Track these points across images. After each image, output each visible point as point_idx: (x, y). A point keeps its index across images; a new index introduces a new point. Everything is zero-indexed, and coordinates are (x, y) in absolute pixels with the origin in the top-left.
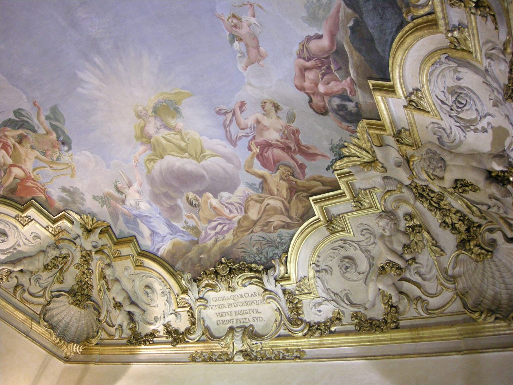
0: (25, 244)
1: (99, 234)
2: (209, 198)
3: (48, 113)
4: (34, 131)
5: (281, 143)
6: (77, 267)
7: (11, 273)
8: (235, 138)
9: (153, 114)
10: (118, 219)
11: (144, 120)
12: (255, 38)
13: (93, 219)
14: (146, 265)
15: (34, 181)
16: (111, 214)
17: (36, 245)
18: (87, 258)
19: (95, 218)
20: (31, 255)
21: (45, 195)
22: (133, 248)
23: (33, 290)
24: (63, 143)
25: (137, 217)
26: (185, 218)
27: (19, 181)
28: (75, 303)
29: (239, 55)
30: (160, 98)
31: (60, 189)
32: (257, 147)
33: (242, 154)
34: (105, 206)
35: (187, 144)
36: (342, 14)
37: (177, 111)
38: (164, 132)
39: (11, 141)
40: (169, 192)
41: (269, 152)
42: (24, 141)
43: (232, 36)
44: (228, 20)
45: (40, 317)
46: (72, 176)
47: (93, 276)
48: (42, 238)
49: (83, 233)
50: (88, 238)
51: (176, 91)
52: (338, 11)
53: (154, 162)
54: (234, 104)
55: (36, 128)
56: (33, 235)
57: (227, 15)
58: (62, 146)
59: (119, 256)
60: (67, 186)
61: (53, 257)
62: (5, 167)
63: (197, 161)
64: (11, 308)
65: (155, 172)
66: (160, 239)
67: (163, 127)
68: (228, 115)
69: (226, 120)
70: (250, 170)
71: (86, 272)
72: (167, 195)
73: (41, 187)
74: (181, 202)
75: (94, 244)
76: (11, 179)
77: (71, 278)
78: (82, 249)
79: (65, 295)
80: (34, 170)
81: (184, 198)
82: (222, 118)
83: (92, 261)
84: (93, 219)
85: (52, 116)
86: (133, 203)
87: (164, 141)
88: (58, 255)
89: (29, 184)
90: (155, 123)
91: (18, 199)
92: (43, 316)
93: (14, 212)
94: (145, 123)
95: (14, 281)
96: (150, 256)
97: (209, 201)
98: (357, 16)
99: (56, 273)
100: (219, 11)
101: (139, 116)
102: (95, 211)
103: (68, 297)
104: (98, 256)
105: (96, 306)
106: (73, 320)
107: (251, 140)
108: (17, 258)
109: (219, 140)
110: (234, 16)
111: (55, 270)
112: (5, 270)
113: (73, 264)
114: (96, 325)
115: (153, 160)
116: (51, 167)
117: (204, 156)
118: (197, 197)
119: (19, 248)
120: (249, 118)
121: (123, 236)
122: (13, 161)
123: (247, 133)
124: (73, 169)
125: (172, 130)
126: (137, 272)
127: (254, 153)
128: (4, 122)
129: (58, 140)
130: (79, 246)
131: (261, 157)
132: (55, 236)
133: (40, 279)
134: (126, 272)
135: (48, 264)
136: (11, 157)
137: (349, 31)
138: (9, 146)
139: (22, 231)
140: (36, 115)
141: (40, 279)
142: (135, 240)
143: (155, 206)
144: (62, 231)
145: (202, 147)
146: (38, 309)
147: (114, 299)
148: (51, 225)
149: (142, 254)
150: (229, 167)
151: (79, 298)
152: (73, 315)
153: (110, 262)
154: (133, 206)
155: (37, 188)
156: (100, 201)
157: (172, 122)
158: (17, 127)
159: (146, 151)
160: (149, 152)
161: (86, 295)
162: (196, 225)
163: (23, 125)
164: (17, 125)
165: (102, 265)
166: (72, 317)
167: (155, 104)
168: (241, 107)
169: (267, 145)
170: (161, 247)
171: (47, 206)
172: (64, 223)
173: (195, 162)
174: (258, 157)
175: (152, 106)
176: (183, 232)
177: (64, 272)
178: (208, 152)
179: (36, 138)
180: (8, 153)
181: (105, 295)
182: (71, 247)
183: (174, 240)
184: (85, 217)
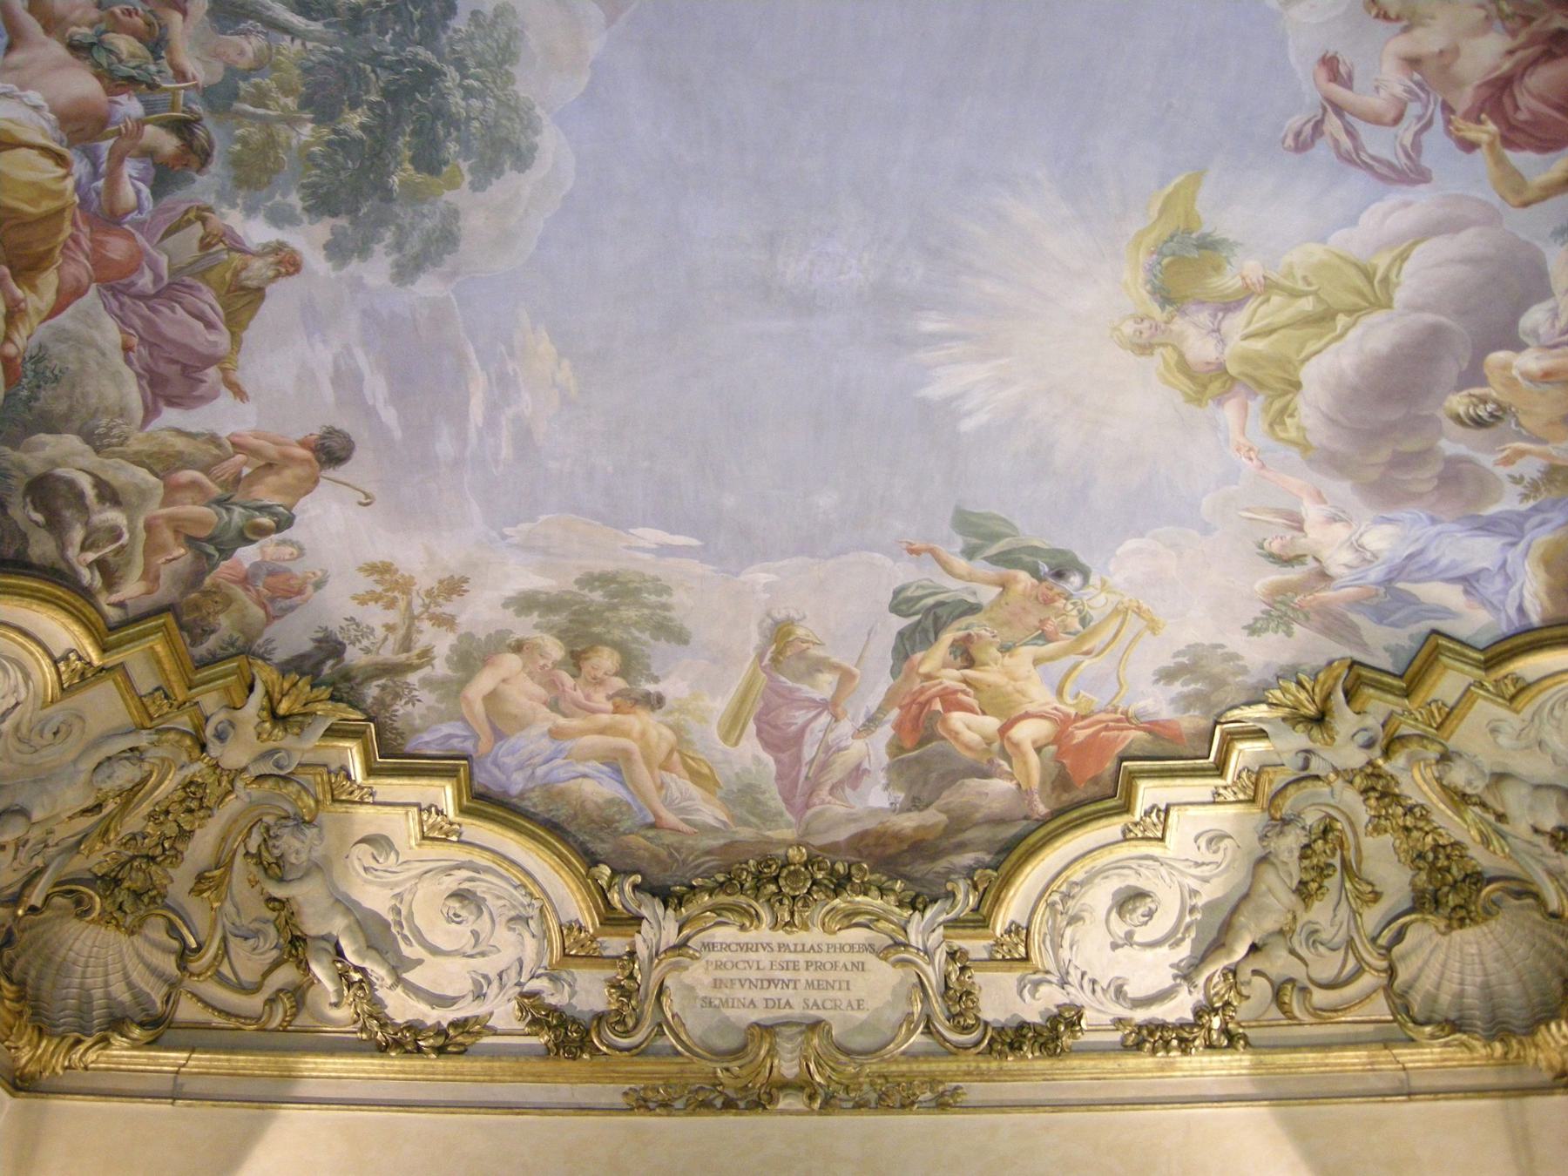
0: (1205, 880)
1: (1348, 702)
2: (1506, 367)
3: (959, 542)
4: (974, 609)
5: (1523, 47)
6: (1378, 830)
7: (1235, 974)
8: (1404, 160)
9: (1169, 308)
10: (1354, 628)
11: (1164, 345)
13: (1300, 684)
14: (1530, 678)
15: (1084, 717)
16: (1327, 631)
17: (1233, 860)
18: (1378, 788)
19: (1302, 677)
20: (1244, 890)
21: (1138, 728)
22: (1458, 665)
23: (1326, 972)
24: (1059, 575)
25: (1390, 580)
26: (1502, 472)
27: (1053, 748)
28: (1455, 923)
30: (1143, 258)
31: (1157, 681)
32: (1479, 122)
33: (1465, 177)
34: (1296, 627)
35: (1315, 293)
37: (1208, 245)
38: (1236, 323)
39: (951, 678)
40: (1400, 448)
41: (1524, 100)
42: (974, 652)
45: (1401, 1025)
46: (1153, 627)
47: (1437, 819)
48: (1229, 832)
49: (1310, 737)
50: (1333, 739)
51: (1157, 205)
53: (1292, 416)
54: (1310, 87)
55: (971, 599)
56: (1203, 842)
58: (1062, 583)
59: (1448, 714)
60: (1169, 662)
61: (1296, 854)
62: (996, 746)
63: (1381, 307)
64: (1311, 1057)
65: (1320, 435)
66: (1499, 583)
67: (1220, 315)
68: (1327, 127)
69: (1336, 142)
70: (1529, 195)
71: (1409, 821)
72: (1402, 462)
73: (1113, 716)
74: (1454, 444)
75: (1362, 738)
76: (1033, 759)
77: (1387, 866)
78: (1348, 776)
79: (1412, 922)
80: (1060, 693)
81: (1449, 424)
82: (1322, 149)
83: (1397, 784)
84: (1300, 684)
85: (974, 541)
86: (1347, 556)
87: (1259, 345)
88: (1305, 841)
89: (1080, 735)
90: (1196, 325)
91: (1094, 790)
92: (1409, 1017)
93: (1111, 829)
94: (1175, 348)
95: (1261, 988)
96: (1518, 646)
97: (1515, 372)
99: (1342, 885)
101: (1145, 349)
102: (1285, 658)
103: (1425, 921)
104: (1399, 760)
105: (1514, 886)
106: (1492, 966)
107: (1448, 122)
108: (1217, 925)
109: (1377, 204)
111: (1332, 883)
112: (1216, 979)
113: (1361, 830)
114: (1557, 931)
115: (1283, 411)
116: (1087, 653)
117: (1385, 280)
118: (1477, 391)
119: (1200, 901)
120: (1381, 76)
121: (1405, 658)
122: (996, 715)
123: (1420, 118)
124: (1139, 612)
125: (1246, 299)
126: (1527, 712)
127: (1491, 145)
128: (895, 649)
129: (1041, 580)
130: (1332, 776)
131: (1514, 135)
132: (1252, 801)
133: (1316, 931)
134: (1503, 740)
135: (1302, 883)
136: (984, 713)
138: (955, 692)
139: (1170, 854)
140: (940, 570)
141: (1316, 931)
142: (1443, 642)
143: (1406, 513)
144: (1259, 774)
145: (1356, 265)
146: (1380, 1008)
147: (1536, 831)
148: (1219, 782)
149: (1492, 658)
150: (1469, 240)
151: (1452, 900)
152: (1480, 954)
153: (1438, 748)
154: (1355, 563)
155: (1107, 728)
156: (1273, 625)
157: (1228, 281)
158: (932, 636)
159: (1245, 408)
160: (1255, 405)
161: (1464, 880)
162: (1545, 462)
163: (937, 619)
164: (925, 631)
165: (1435, 771)
166: (1482, 963)
167: (1147, 282)
168: (1335, 76)
169: (1498, 94)
170: (1522, 596)
171: (1170, 748)
172: (1245, 753)
173: (1378, 316)
174: (1508, 143)
175: (1147, 296)
176: (1535, 509)
177: (1359, 869)
178: (1382, 262)
179: (990, 619)
180: (971, 710)
181: (1510, 839)
182: (1319, 795)
183: (1536, 552)
184: (1278, 693)
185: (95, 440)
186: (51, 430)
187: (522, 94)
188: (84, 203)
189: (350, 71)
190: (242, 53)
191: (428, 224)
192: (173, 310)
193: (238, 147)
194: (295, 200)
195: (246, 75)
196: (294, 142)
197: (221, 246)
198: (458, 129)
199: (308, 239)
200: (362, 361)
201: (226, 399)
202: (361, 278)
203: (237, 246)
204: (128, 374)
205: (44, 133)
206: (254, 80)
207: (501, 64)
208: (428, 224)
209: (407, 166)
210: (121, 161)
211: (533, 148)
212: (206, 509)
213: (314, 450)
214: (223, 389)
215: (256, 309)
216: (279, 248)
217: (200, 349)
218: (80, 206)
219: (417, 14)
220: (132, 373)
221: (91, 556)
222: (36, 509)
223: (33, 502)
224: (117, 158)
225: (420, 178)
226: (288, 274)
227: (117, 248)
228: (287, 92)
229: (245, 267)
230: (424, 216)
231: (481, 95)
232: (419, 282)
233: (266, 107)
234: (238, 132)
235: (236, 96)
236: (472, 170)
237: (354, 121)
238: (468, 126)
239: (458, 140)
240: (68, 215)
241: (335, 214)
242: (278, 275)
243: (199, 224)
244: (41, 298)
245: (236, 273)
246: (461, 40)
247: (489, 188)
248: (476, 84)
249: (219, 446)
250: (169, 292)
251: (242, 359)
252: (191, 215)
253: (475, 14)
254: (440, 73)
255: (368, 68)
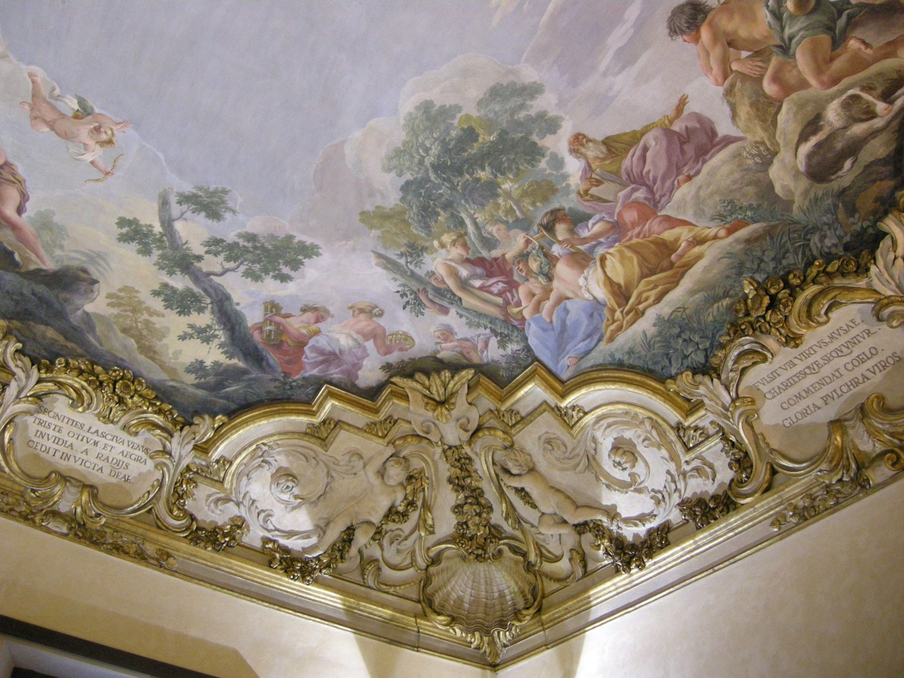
12: (66, 136)
29: (57, 92)
36: (33, 257)
43: (89, 110)
44: (111, 129)
52: (38, 256)
57: (119, 137)
98: (23, 270)
100: (130, 131)
110: (110, 142)
137: (10, 248)
185: (767, 158)
186: (771, 187)
187: (404, 133)
188: (616, 241)
189: (467, 192)
190: (499, 229)
191: (497, 107)
192: (649, 171)
193: (538, 204)
194: (543, 164)
195: (506, 223)
196: (516, 186)
197: (594, 176)
198: (445, 139)
199: (558, 143)
200: (606, 61)
201: (692, 107)
202: (556, 105)
203: (589, 168)
204: (706, 169)
205: (596, 269)
206: (505, 219)
207: (404, 151)
208: (497, 107)
209: (480, 140)
210: (584, 238)
211: (417, 108)
212: (798, 55)
213: (698, 28)
214: (685, 113)
215: (618, 136)
216: (574, 151)
217: (664, 143)
218: (620, 241)
219: (423, 191)
220: (705, 166)
221: (880, 106)
222: (841, 169)
223: (833, 174)
224: (585, 240)
225: (480, 131)
226: (584, 136)
227: (630, 216)
228: (498, 206)
229: (597, 158)
230: (495, 113)
231: (422, 145)
232: (533, 80)
233: (511, 207)
234: (531, 208)
235: (517, 220)
236: (454, 117)
237: (484, 175)
238: (439, 137)
239: (448, 134)
240: (628, 244)
241: (535, 144)
242: (589, 140)
243: (590, 192)
244: (681, 234)
245: (603, 159)
246: (413, 170)
247: (453, 103)
248: (421, 151)
249: (732, 86)
250: (639, 180)
251: (656, 118)
252: (588, 198)
253: (400, 175)
254: (432, 165)
255: (459, 188)
